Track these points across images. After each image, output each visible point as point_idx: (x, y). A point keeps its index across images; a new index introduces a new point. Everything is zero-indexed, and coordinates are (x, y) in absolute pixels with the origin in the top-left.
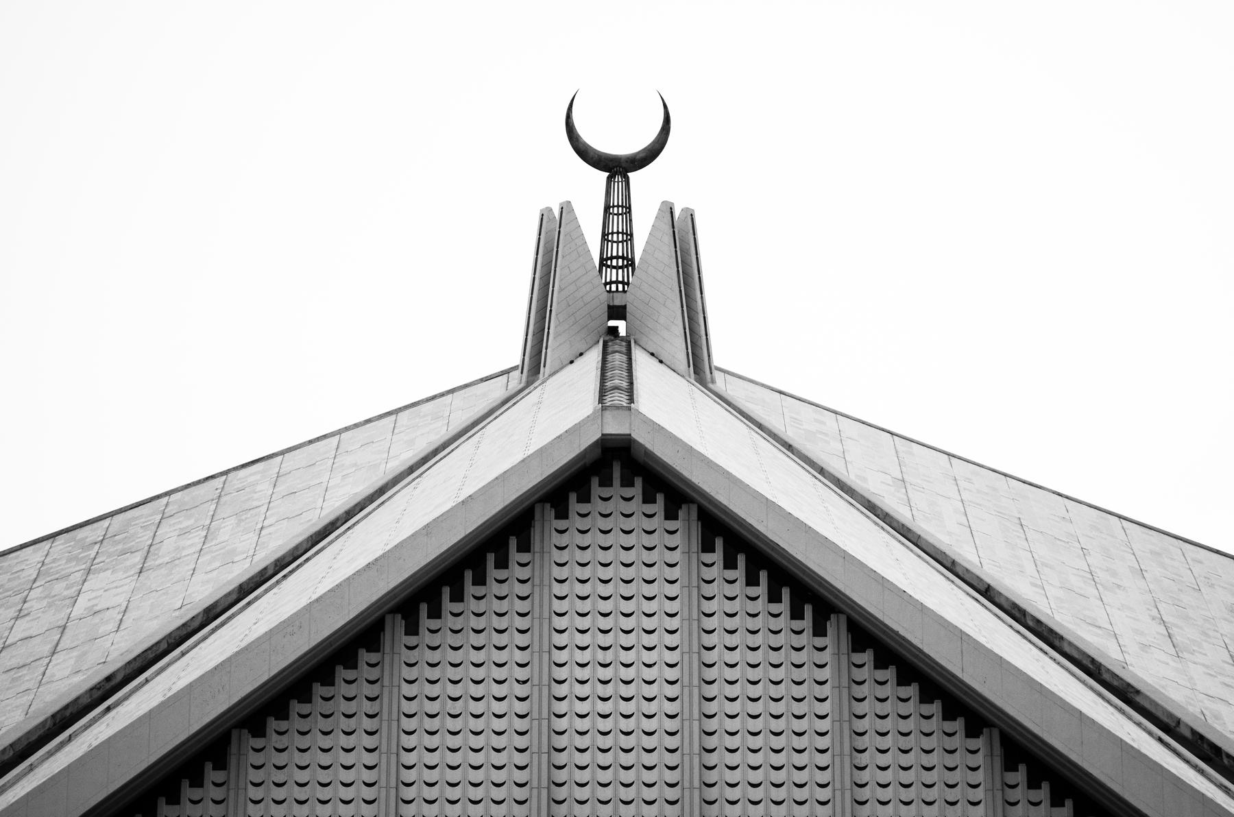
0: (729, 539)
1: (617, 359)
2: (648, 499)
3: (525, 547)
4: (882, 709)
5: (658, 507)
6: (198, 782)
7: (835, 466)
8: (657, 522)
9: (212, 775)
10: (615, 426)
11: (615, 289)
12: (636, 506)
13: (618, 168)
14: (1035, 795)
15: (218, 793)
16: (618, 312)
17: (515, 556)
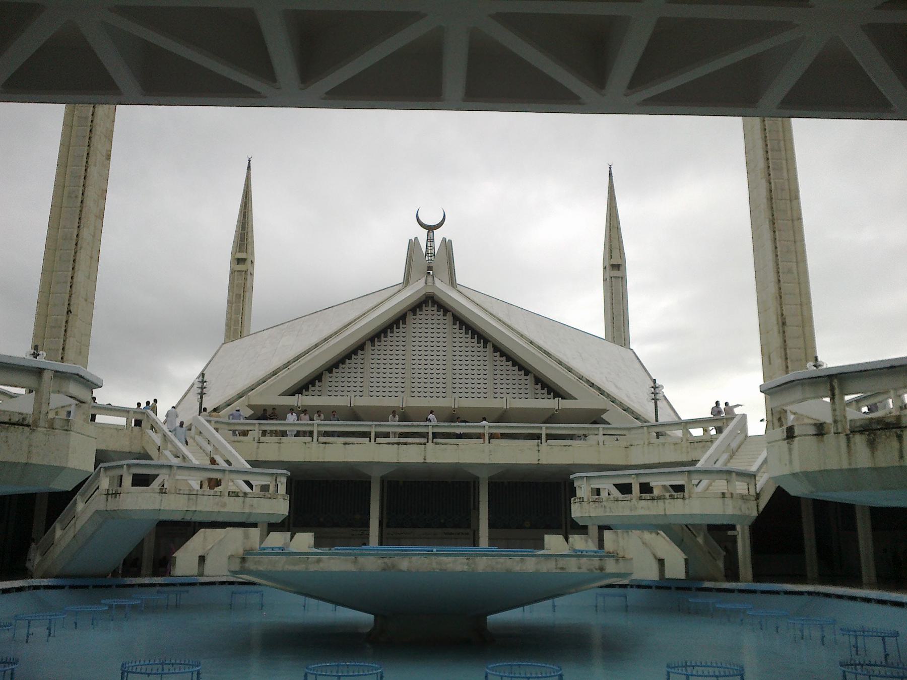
1: (430, 279)
3: (404, 323)
4: (502, 368)
5: (441, 313)
6: (314, 385)
7: (490, 310)
8: (441, 317)
9: (317, 383)
10: (429, 290)
11: (430, 258)
12: (435, 312)
13: (431, 229)
14: (543, 391)
15: (320, 389)
16: (430, 268)
17: (401, 326)
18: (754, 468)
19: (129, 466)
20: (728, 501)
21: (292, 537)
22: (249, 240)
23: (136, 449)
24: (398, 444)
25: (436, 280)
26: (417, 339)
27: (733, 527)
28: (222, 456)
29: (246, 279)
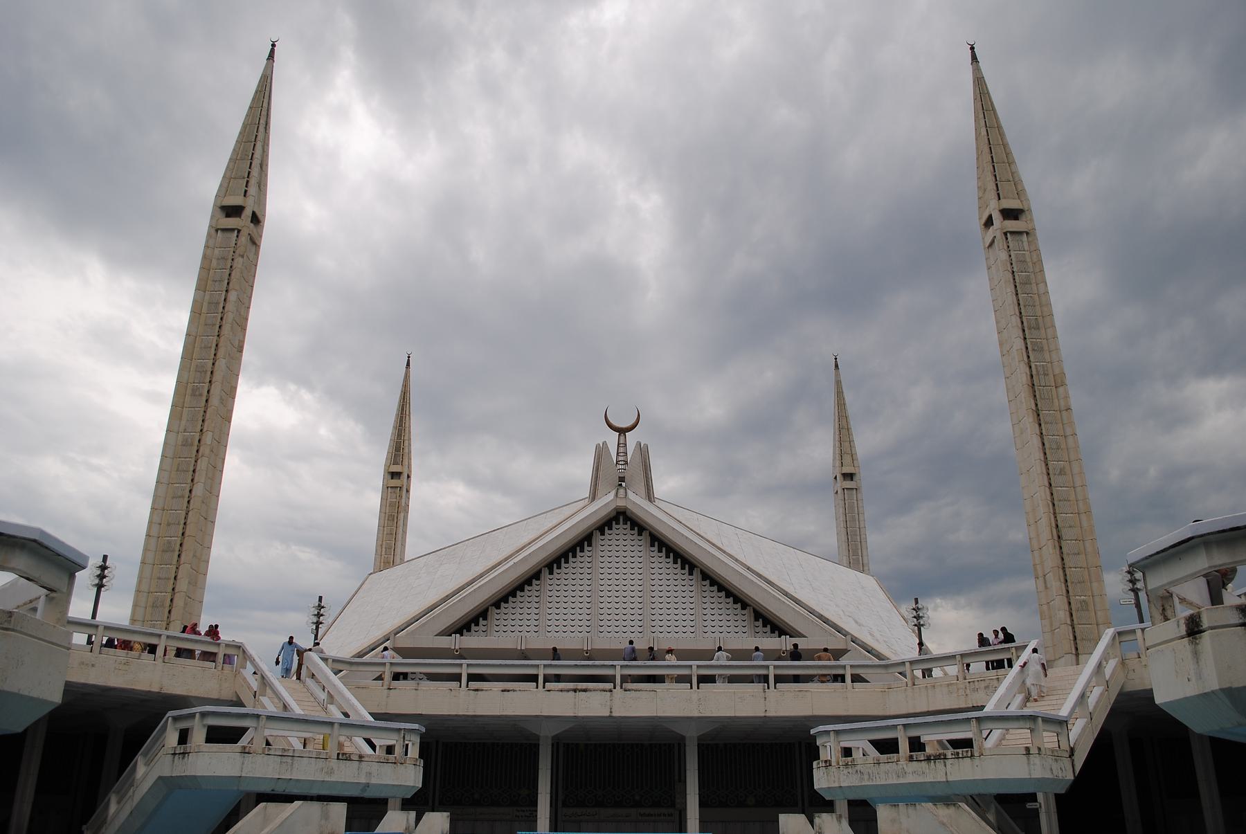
0: (661, 544)
2: (632, 529)
3: (590, 545)
6: (477, 624)
9: (482, 622)
10: (621, 503)
12: (628, 531)
13: (622, 431)
14: (765, 629)
17: (586, 548)
18: (1064, 712)
19: (204, 715)
20: (1035, 759)
21: (418, 819)
22: (406, 450)
23: (227, 694)
24: (575, 691)
25: (630, 494)
26: (606, 565)
27: (1033, 797)
28: (340, 707)
29: (401, 496)
